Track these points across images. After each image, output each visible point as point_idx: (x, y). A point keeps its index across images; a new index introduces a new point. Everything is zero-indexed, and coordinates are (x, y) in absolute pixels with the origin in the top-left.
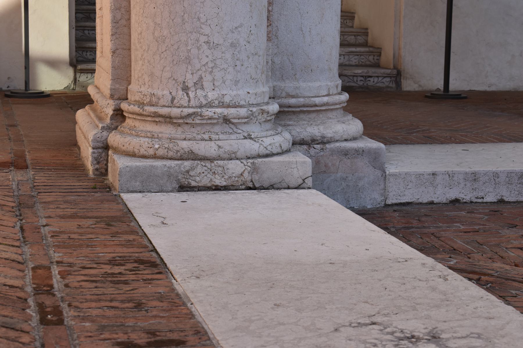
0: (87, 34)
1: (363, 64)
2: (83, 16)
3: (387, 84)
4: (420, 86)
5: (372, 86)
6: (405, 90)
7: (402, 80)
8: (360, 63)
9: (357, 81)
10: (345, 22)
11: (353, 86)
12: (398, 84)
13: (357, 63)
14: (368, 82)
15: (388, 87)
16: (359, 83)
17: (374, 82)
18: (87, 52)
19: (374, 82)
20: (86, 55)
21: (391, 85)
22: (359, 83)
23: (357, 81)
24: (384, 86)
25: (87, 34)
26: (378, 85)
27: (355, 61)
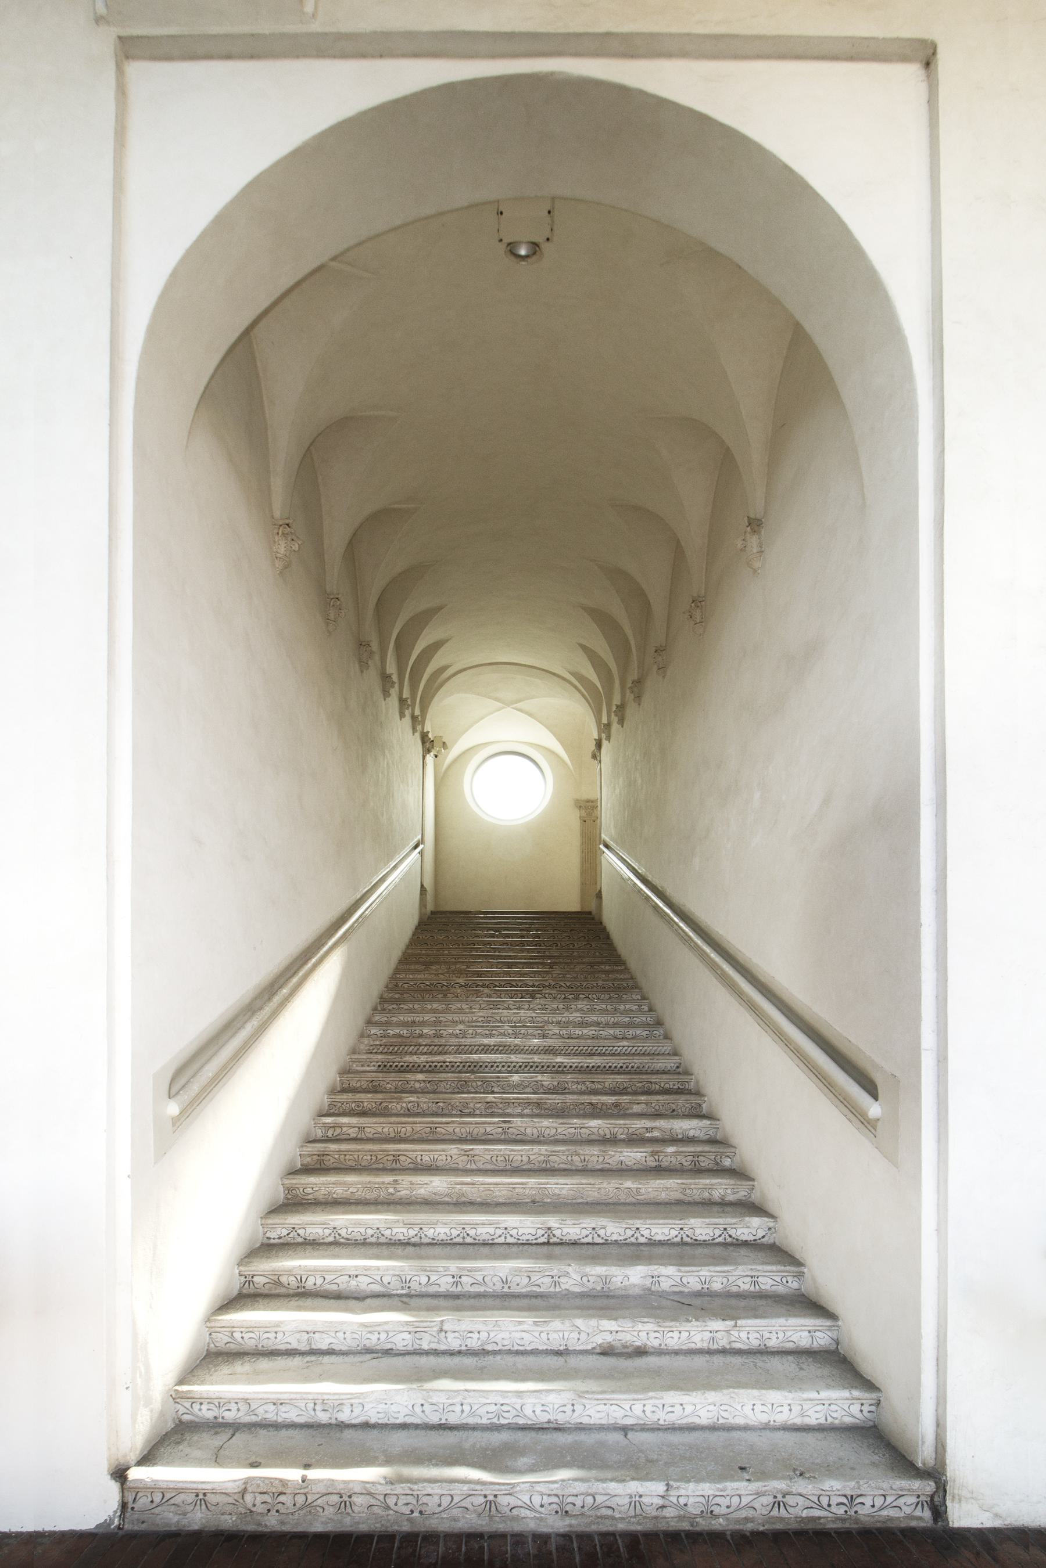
0: (240, 1340)
1: (837, 1422)
2: (268, 1280)
3: (908, 1510)
4: (996, 1515)
5: (868, 1515)
6: (956, 1525)
7: (948, 1503)
8: (830, 1420)
9: (829, 1505)
10: (784, 1280)
11: (820, 1518)
12: (938, 1511)
13: (822, 1421)
14: (858, 1508)
15: (911, 1517)
16: (834, 1509)
17: (873, 1506)
18: (201, 1404)
19: (873, 1506)
20: (200, 1410)
21: (918, 1513)
22: (834, 1509)
23: (829, 1505)
24: (902, 1515)
25: (240, 1340)
26: (885, 1513)
27: (818, 1415)
